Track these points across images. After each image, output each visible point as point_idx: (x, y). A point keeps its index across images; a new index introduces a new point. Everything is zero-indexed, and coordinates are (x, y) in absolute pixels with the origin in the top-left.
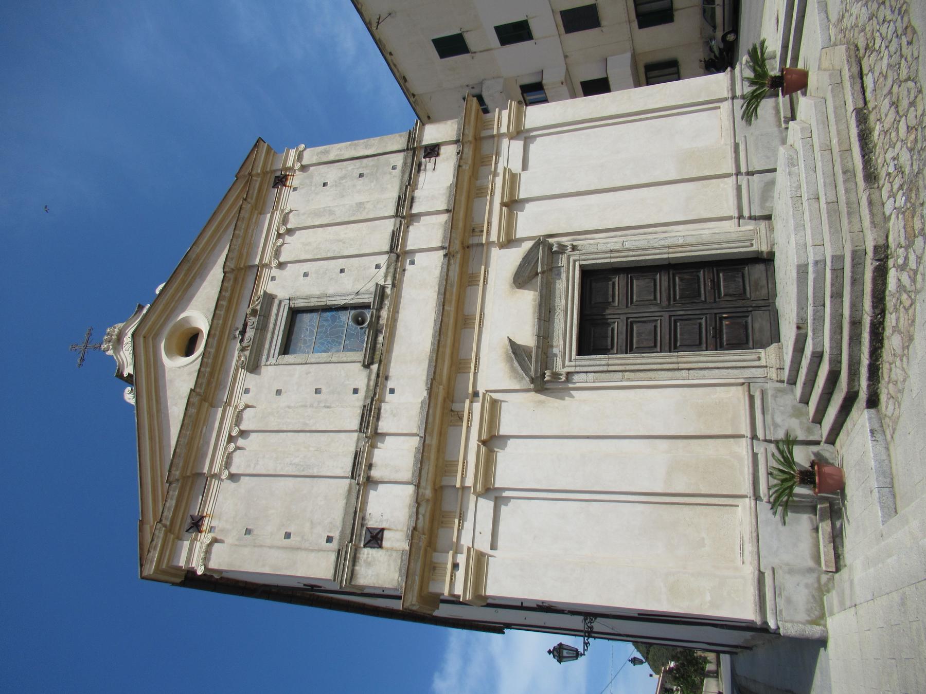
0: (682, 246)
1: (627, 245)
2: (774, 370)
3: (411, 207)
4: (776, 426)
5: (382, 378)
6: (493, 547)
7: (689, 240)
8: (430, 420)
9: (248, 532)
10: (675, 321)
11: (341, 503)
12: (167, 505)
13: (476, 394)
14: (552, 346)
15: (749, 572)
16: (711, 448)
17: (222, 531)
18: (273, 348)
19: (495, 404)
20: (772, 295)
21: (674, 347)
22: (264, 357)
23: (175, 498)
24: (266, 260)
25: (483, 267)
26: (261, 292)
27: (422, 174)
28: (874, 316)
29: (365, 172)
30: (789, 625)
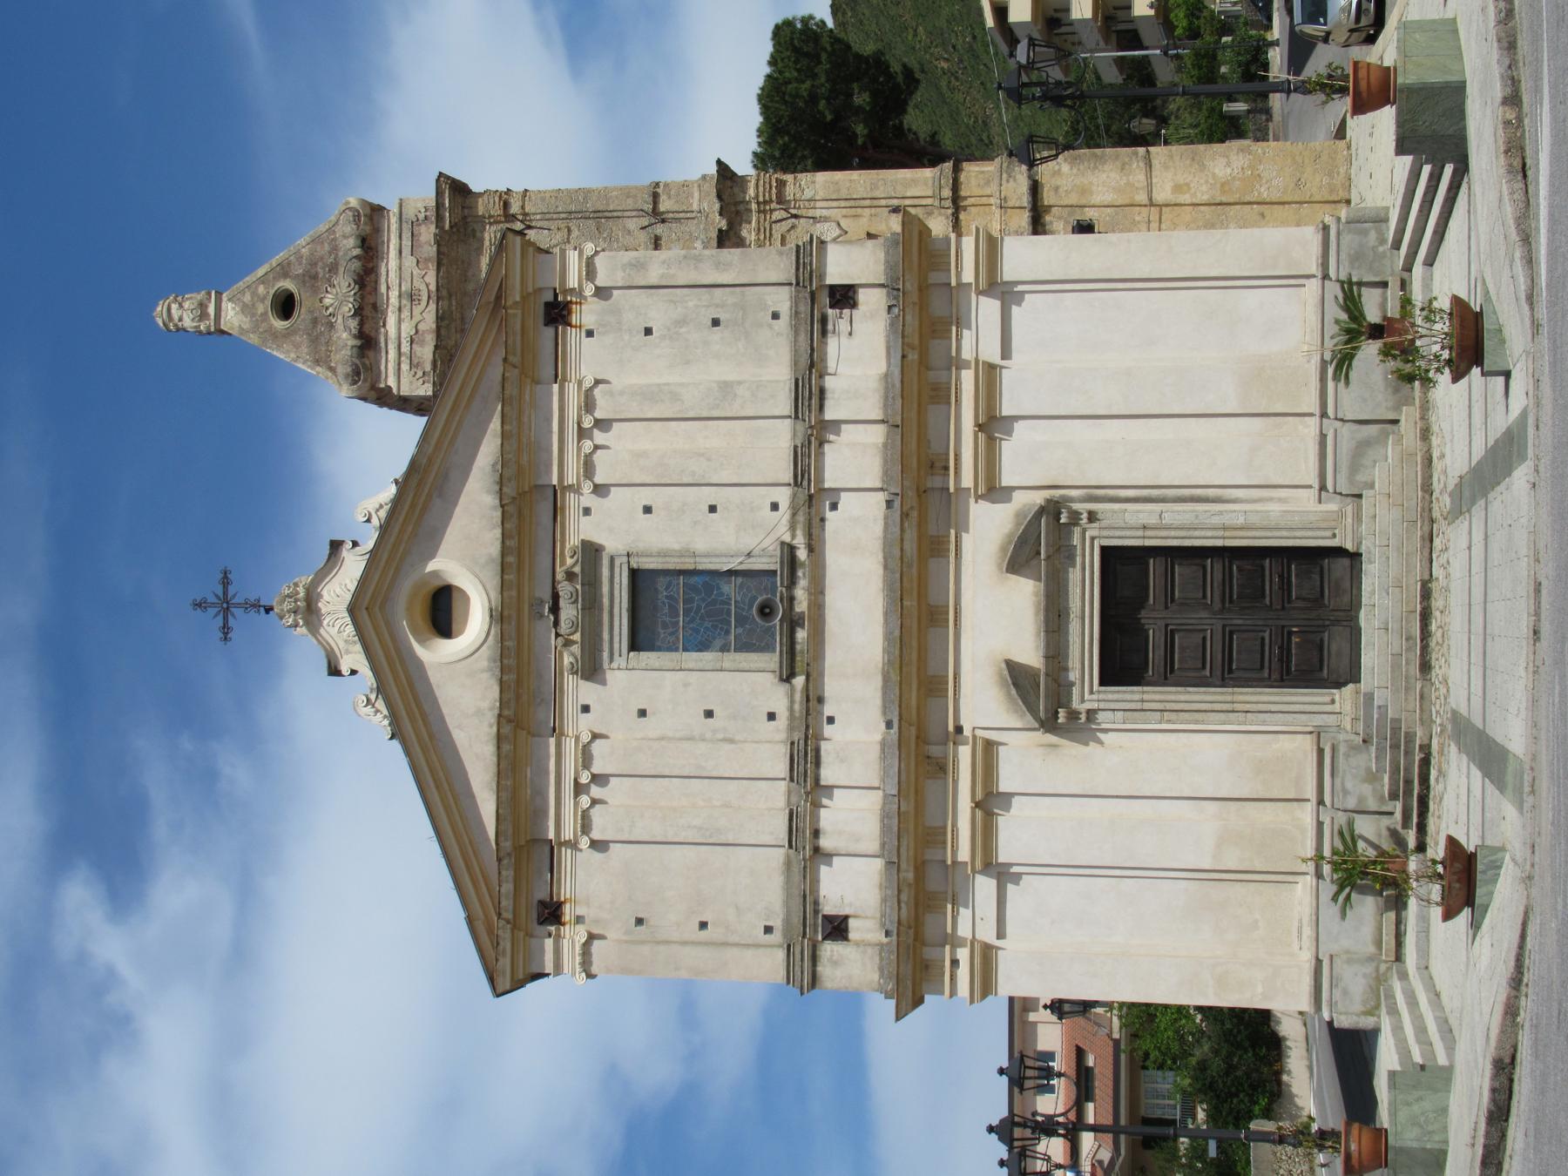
0: (1241, 529)
1: (1168, 519)
2: (1348, 719)
3: (821, 408)
4: (1345, 792)
5: (813, 699)
6: (1001, 934)
7: (1254, 519)
8: (903, 777)
9: (639, 921)
10: (1231, 633)
11: (777, 881)
12: (503, 890)
14: (1066, 669)
15: (1306, 957)
16: (1268, 815)
17: (597, 921)
18: (616, 639)
19: (990, 747)
20: (1355, 605)
21: (1228, 673)
22: (606, 655)
23: (511, 879)
24: (571, 479)
25: (953, 532)
26: (573, 541)
27: (832, 343)
28: (1421, 790)
29: (722, 317)
30: (1343, 1018)
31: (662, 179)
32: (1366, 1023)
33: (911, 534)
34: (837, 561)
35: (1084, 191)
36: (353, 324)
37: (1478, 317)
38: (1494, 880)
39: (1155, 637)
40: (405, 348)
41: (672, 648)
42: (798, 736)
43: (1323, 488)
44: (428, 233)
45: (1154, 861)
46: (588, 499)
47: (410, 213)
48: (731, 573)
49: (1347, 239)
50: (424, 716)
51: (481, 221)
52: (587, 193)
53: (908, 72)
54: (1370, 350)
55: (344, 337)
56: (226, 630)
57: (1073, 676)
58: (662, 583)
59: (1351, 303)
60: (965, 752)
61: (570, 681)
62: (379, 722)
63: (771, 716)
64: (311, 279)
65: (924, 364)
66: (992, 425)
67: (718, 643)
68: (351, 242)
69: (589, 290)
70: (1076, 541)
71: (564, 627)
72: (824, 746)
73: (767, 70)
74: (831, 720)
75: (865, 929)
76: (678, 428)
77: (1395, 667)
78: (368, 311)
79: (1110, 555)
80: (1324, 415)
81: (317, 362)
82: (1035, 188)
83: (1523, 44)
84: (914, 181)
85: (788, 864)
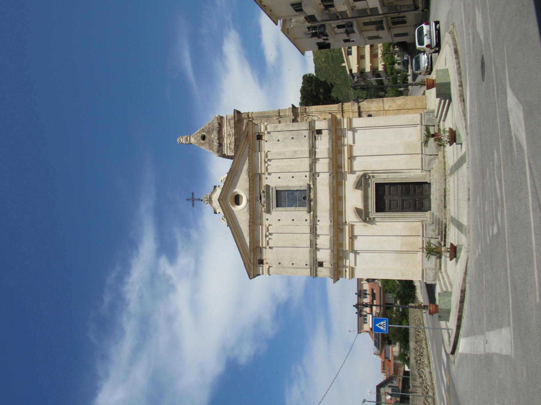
1: (389, 177)
3: (315, 155)
5: (315, 216)
6: (355, 265)
7: (408, 176)
9: (279, 263)
11: (308, 255)
13: (346, 222)
14: (368, 209)
15: (420, 269)
19: (352, 226)
21: (403, 209)
24: (263, 172)
27: (317, 142)
31: (281, 108)
32: (434, 283)
33: (335, 182)
34: (319, 187)
35: (370, 108)
36: (217, 141)
37: (455, 132)
38: (461, 252)
39: (387, 202)
40: (228, 146)
41: (285, 207)
42: (312, 224)
43: (422, 169)
44: (232, 122)
45: (388, 249)
46: (267, 176)
47: (228, 118)
48: (297, 190)
49: (426, 116)
51: (243, 119)
52: (265, 112)
53: (331, 84)
54: (432, 140)
55: (216, 144)
56: (193, 205)
57: (370, 210)
58: (283, 193)
59: (427, 130)
60: (347, 227)
61: (264, 214)
62: (225, 223)
64: (209, 132)
65: (337, 145)
66: (351, 158)
68: (217, 124)
69: (266, 132)
70: (370, 182)
71: (262, 203)
72: (317, 226)
74: (319, 221)
75: (327, 264)
76: (285, 160)
77: (439, 207)
78: (220, 138)
79: (377, 184)
80: (422, 154)
81: (210, 149)
82: (359, 108)
83: (463, 74)
85: (310, 251)
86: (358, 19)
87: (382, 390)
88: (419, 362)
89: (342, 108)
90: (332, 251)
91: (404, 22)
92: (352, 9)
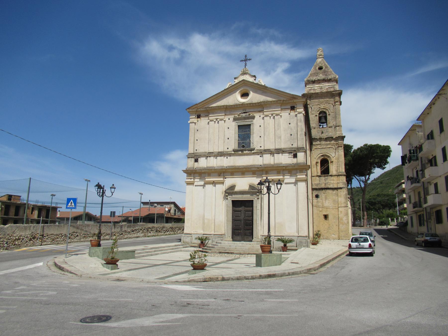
3: (276, 153)
5: (230, 155)
7: (258, 225)
9: (198, 130)
13: (226, 178)
15: (192, 232)
16: (213, 227)
19: (223, 183)
20: (245, 241)
21: (234, 220)
26: (255, 114)
27: (287, 154)
31: (342, 128)
33: (255, 169)
34: (252, 157)
35: (340, 196)
36: (317, 79)
38: (107, 268)
39: (240, 209)
40: (313, 88)
42: (225, 153)
45: (206, 210)
46: (262, 116)
49: (304, 240)
50: (228, 94)
52: (340, 115)
54: (282, 244)
55: (314, 78)
56: (242, 61)
57: (233, 196)
59: (291, 241)
60: (222, 179)
61: (233, 116)
63: (228, 148)
65: (283, 170)
67: (240, 139)
69: (296, 113)
71: (241, 114)
73: (382, 145)
77: (223, 248)
81: (311, 74)
82: (341, 188)
84: (342, 168)
85: (206, 152)
86: (422, 187)
87: (172, 206)
88: (150, 229)
89: (341, 175)
90: (205, 169)
91: (420, 225)
92: (429, 183)
